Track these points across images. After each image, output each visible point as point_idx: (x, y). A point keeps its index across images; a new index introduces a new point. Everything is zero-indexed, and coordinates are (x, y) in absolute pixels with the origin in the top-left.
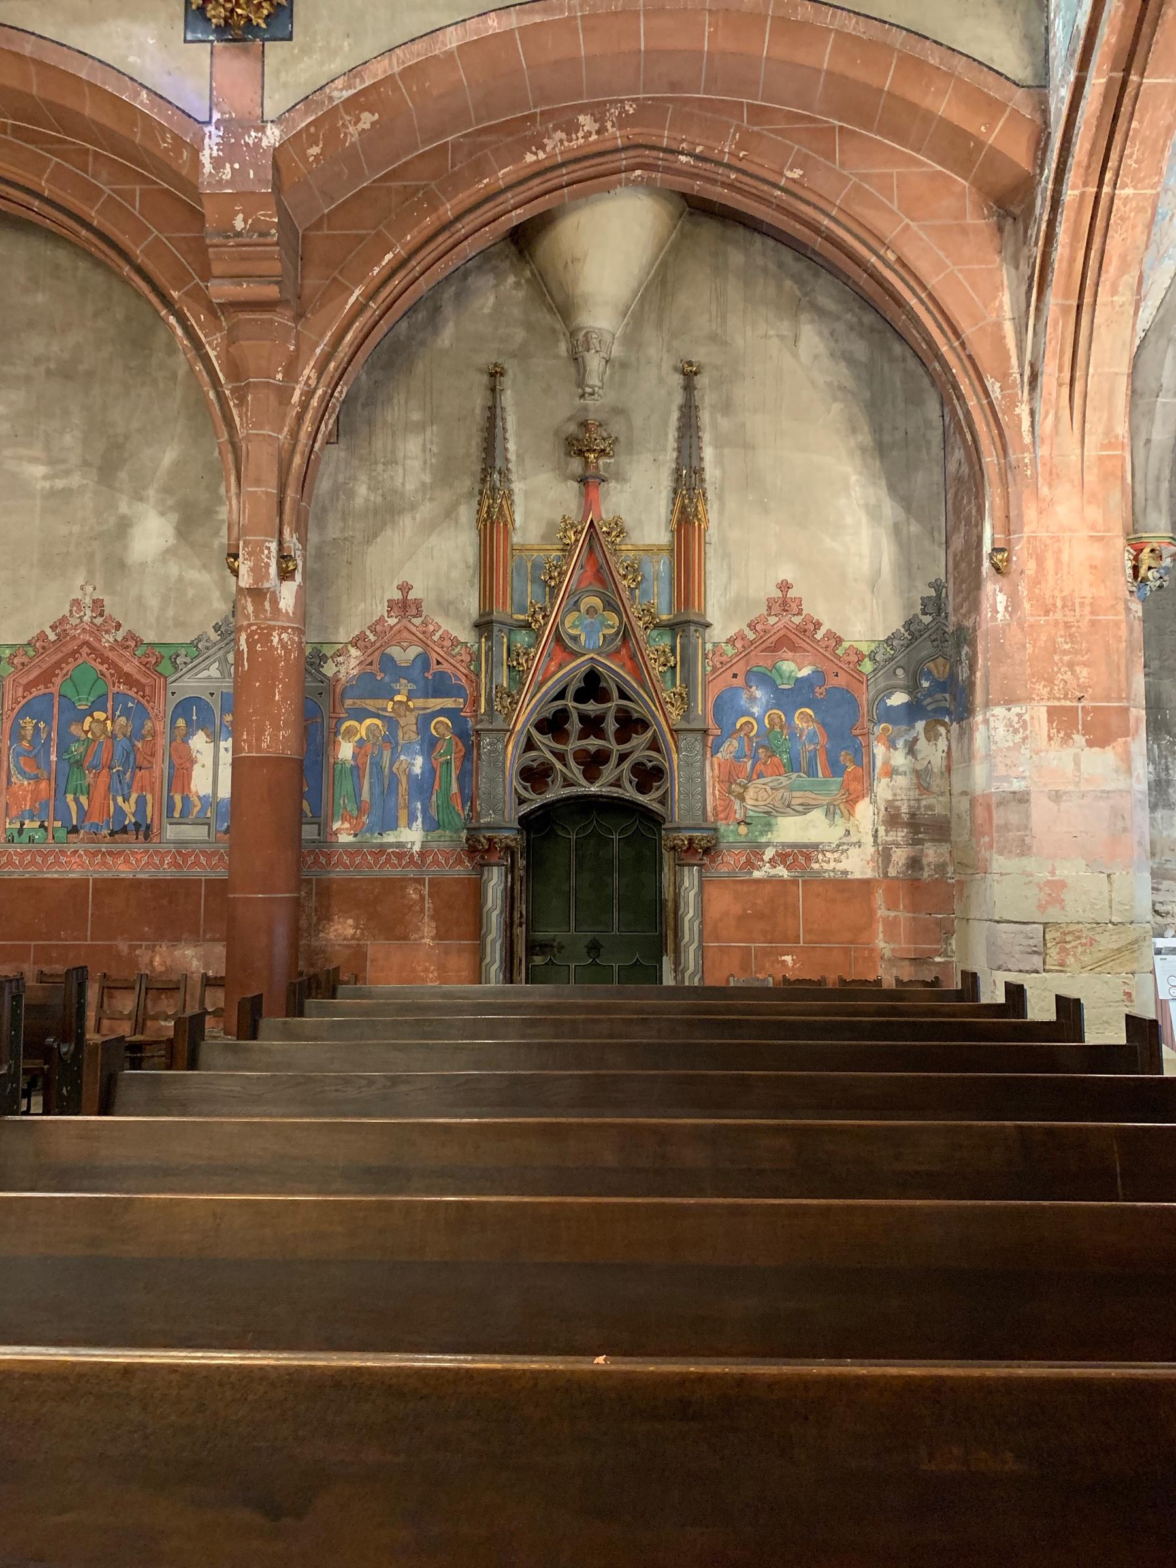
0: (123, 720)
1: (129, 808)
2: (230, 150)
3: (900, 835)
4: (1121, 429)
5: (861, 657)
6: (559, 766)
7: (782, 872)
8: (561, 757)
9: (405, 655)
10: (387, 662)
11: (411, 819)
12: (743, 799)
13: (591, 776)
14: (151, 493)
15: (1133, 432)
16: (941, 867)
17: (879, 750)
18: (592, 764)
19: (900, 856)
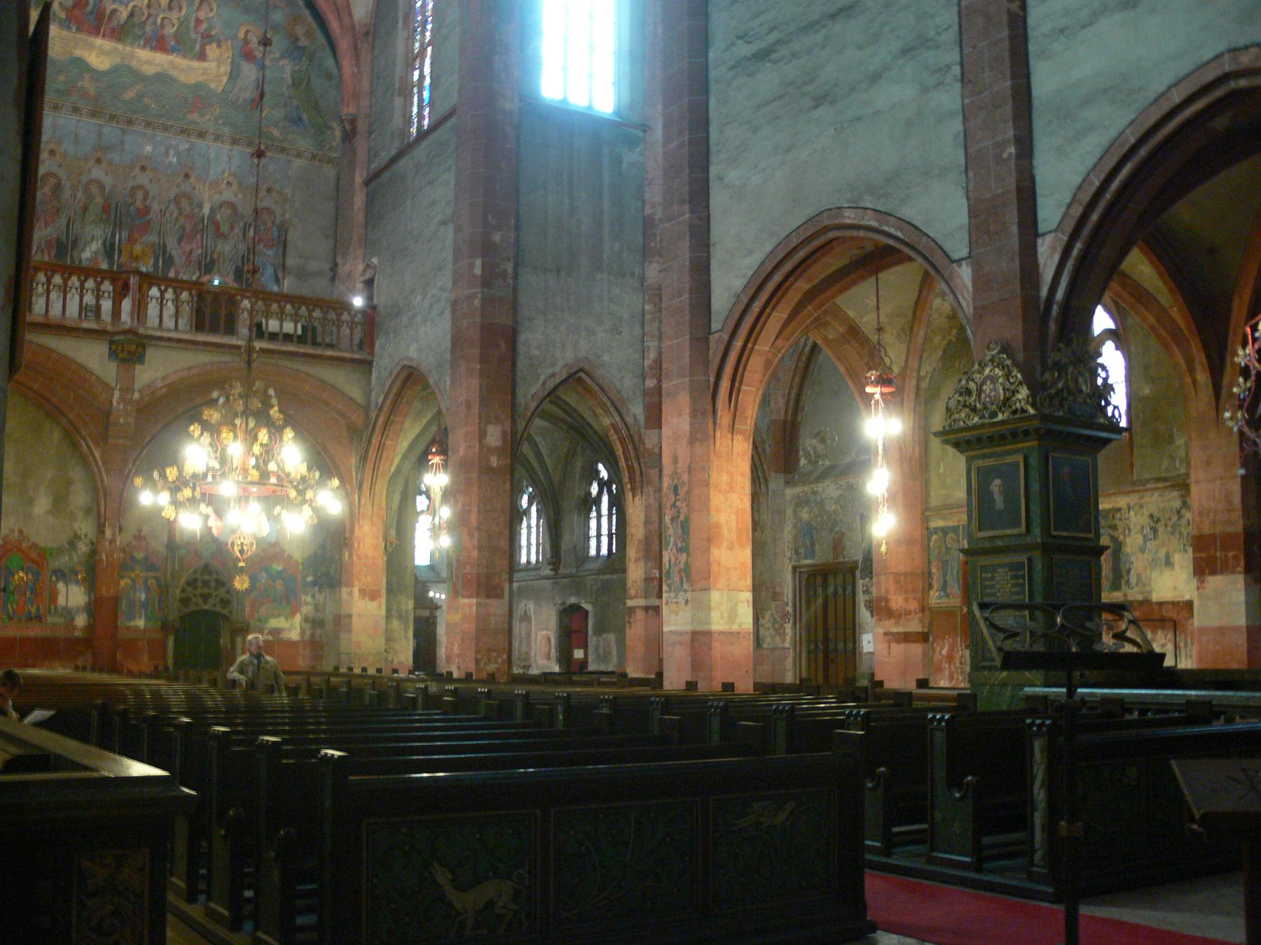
0: (30, 577)
1: (33, 610)
2: (122, 399)
3: (308, 626)
4: (384, 504)
5: (298, 562)
6: (194, 599)
7: (270, 638)
8: (195, 595)
9: (140, 555)
10: (133, 558)
11: (140, 618)
12: (257, 612)
13: (205, 602)
14: (42, 488)
15: (387, 505)
16: (321, 637)
17: (303, 597)
18: (206, 597)
19: (308, 633)
